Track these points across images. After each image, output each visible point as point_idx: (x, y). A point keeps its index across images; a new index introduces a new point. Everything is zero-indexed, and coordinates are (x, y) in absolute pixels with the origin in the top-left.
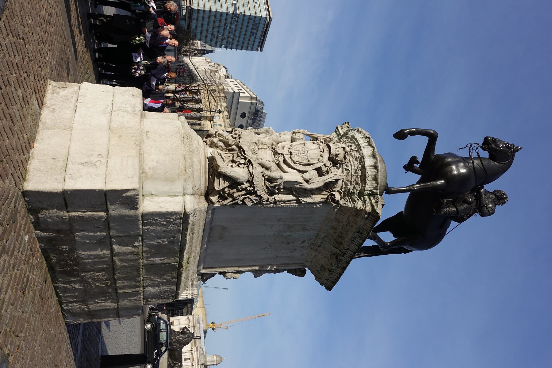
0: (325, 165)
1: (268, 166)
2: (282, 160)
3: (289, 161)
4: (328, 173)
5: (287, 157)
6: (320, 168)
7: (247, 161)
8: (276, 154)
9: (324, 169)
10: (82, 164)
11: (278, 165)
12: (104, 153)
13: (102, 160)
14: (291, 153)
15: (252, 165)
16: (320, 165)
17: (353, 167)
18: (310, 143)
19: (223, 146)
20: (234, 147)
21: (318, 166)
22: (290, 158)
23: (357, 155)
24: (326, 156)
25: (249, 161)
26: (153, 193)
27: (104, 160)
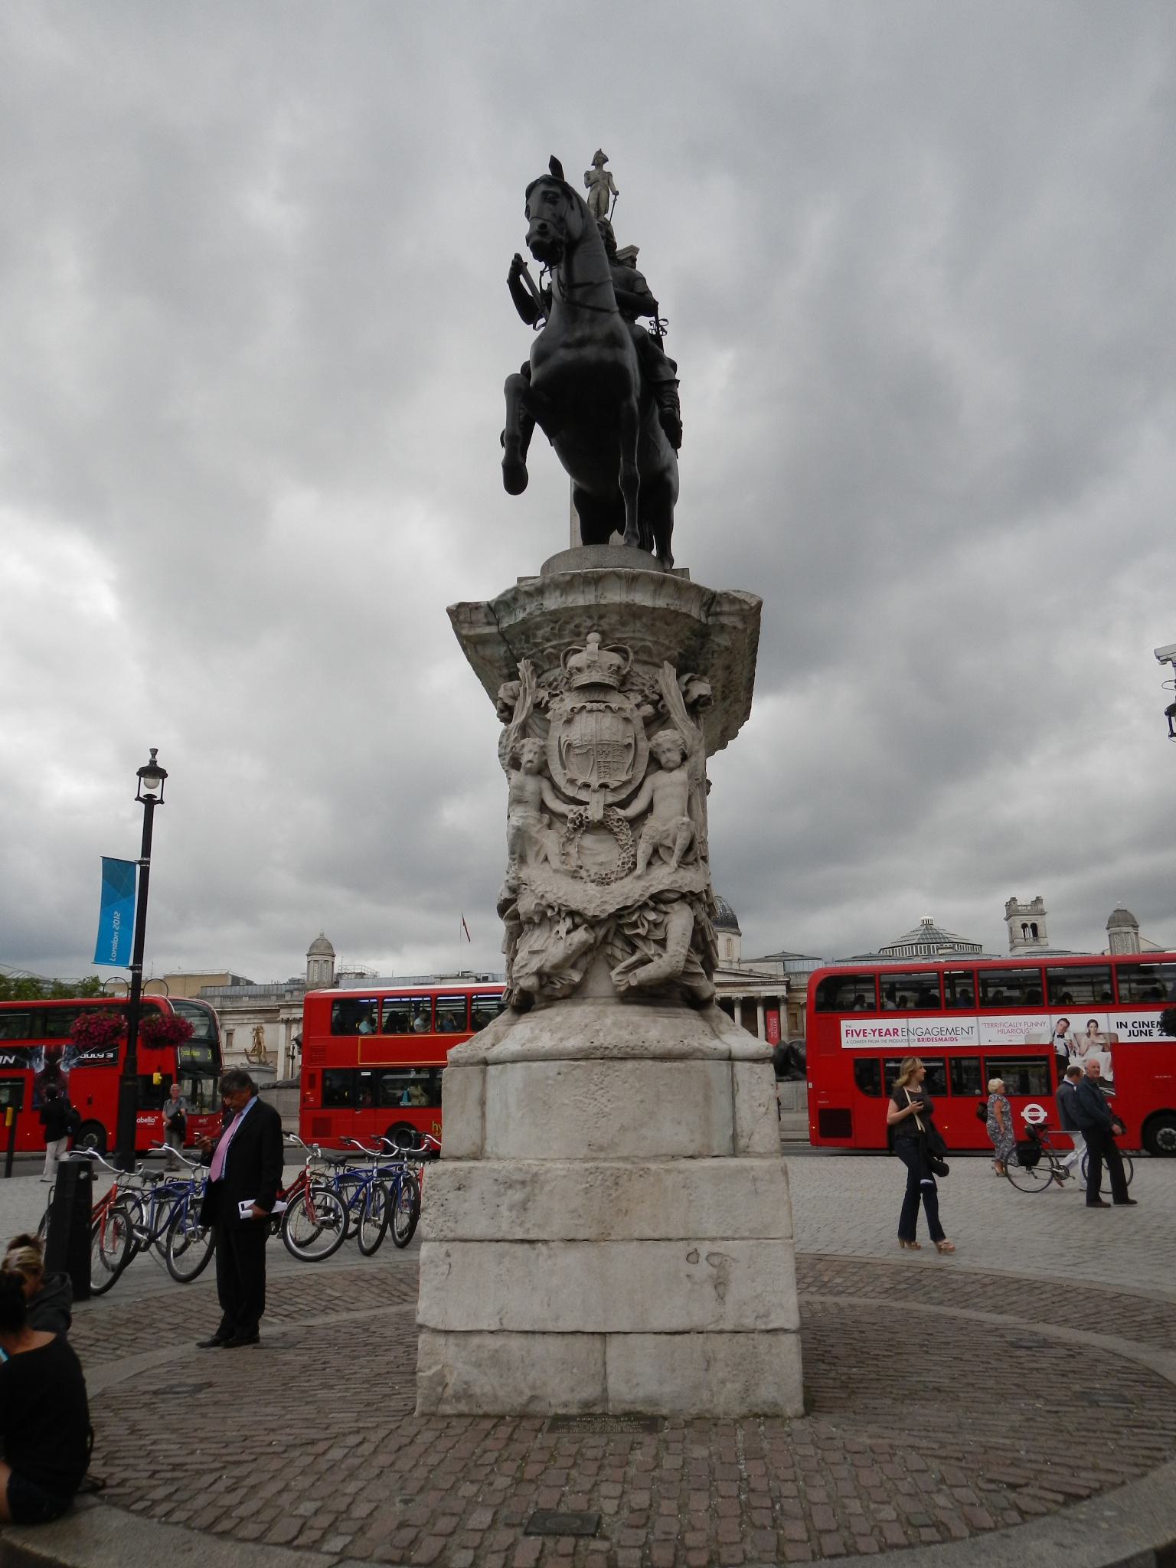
0: (638, 706)
1: (650, 850)
2: (621, 813)
3: (623, 795)
4: (658, 701)
5: (611, 798)
6: (644, 718)
7: (651, 904)
8: (601, 827)
9: (648, 709)
10: (721, 1298)
11: (636, 821)
12: (682, 1248)
13: (703, 1255)
14: (604, 786)
15: (662, 892)
16: (638, 716)
17: (638, 635)
18: (559, 734)
19: (589, 958)
20: (601, 932)
21: (639, 723)
22: (614, 790)
23: (615, 618)
24: (615, 700)
25: (652, 897)
26: (731, 1132)
27: (705, 1248)
